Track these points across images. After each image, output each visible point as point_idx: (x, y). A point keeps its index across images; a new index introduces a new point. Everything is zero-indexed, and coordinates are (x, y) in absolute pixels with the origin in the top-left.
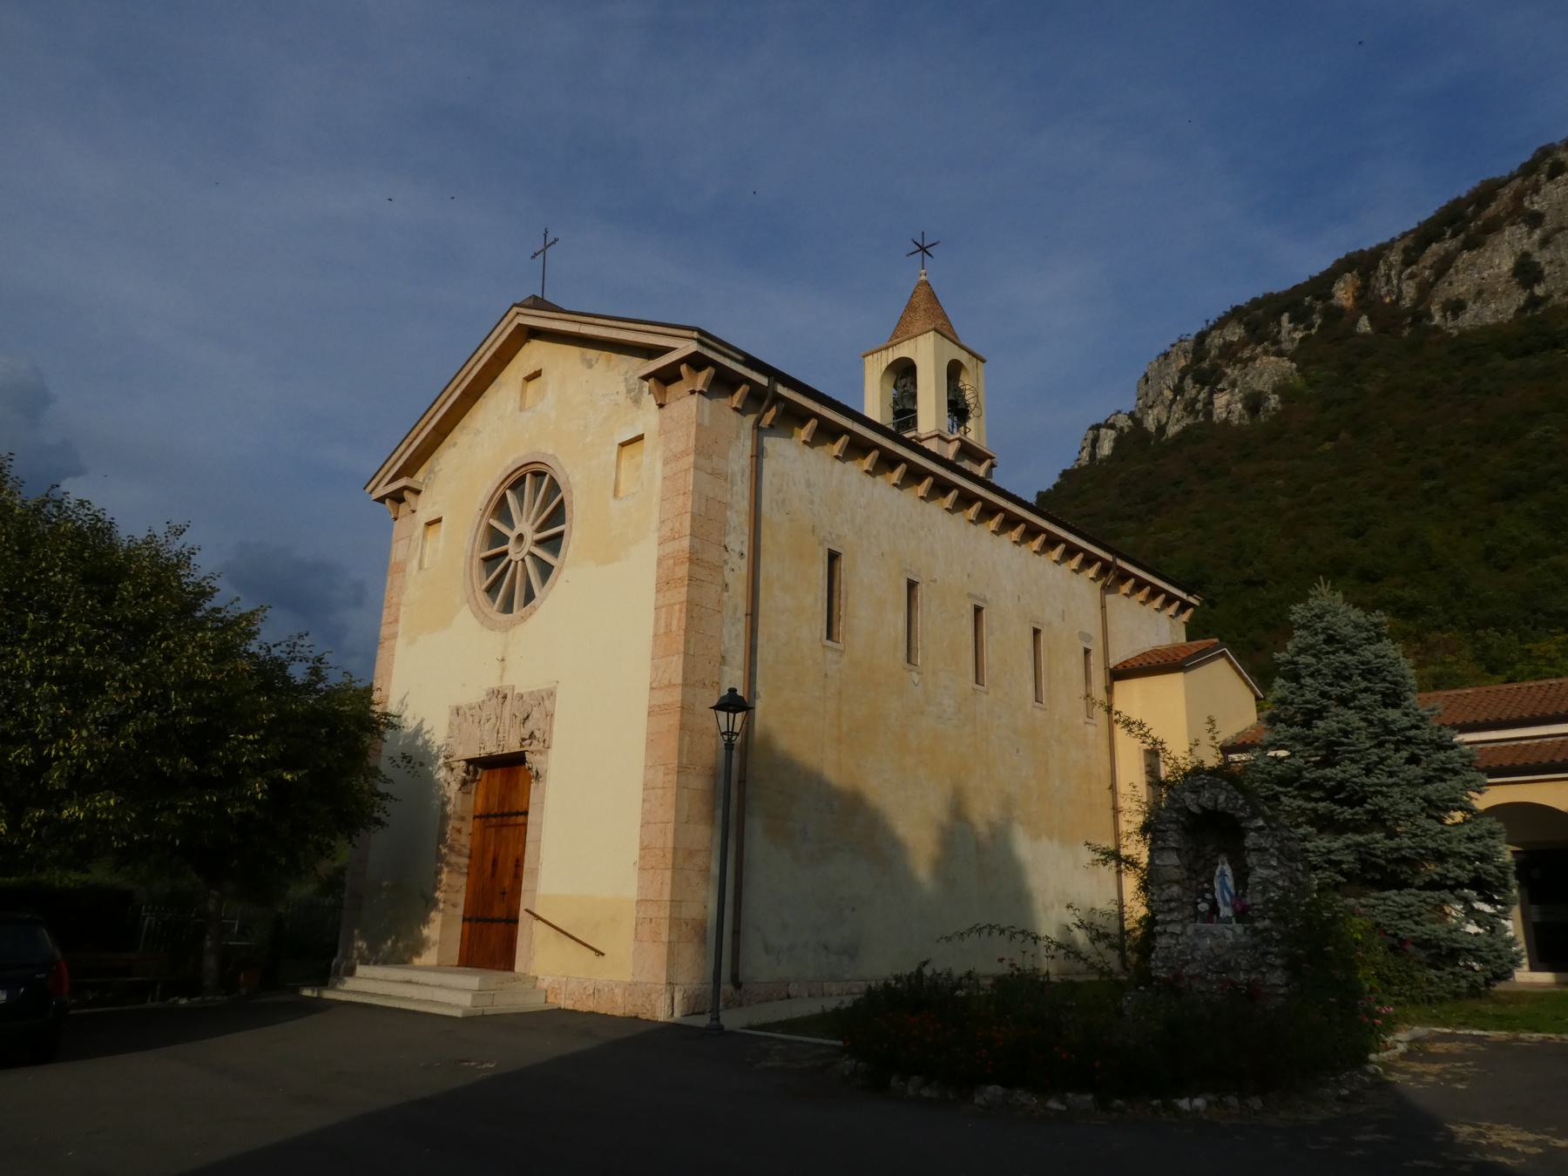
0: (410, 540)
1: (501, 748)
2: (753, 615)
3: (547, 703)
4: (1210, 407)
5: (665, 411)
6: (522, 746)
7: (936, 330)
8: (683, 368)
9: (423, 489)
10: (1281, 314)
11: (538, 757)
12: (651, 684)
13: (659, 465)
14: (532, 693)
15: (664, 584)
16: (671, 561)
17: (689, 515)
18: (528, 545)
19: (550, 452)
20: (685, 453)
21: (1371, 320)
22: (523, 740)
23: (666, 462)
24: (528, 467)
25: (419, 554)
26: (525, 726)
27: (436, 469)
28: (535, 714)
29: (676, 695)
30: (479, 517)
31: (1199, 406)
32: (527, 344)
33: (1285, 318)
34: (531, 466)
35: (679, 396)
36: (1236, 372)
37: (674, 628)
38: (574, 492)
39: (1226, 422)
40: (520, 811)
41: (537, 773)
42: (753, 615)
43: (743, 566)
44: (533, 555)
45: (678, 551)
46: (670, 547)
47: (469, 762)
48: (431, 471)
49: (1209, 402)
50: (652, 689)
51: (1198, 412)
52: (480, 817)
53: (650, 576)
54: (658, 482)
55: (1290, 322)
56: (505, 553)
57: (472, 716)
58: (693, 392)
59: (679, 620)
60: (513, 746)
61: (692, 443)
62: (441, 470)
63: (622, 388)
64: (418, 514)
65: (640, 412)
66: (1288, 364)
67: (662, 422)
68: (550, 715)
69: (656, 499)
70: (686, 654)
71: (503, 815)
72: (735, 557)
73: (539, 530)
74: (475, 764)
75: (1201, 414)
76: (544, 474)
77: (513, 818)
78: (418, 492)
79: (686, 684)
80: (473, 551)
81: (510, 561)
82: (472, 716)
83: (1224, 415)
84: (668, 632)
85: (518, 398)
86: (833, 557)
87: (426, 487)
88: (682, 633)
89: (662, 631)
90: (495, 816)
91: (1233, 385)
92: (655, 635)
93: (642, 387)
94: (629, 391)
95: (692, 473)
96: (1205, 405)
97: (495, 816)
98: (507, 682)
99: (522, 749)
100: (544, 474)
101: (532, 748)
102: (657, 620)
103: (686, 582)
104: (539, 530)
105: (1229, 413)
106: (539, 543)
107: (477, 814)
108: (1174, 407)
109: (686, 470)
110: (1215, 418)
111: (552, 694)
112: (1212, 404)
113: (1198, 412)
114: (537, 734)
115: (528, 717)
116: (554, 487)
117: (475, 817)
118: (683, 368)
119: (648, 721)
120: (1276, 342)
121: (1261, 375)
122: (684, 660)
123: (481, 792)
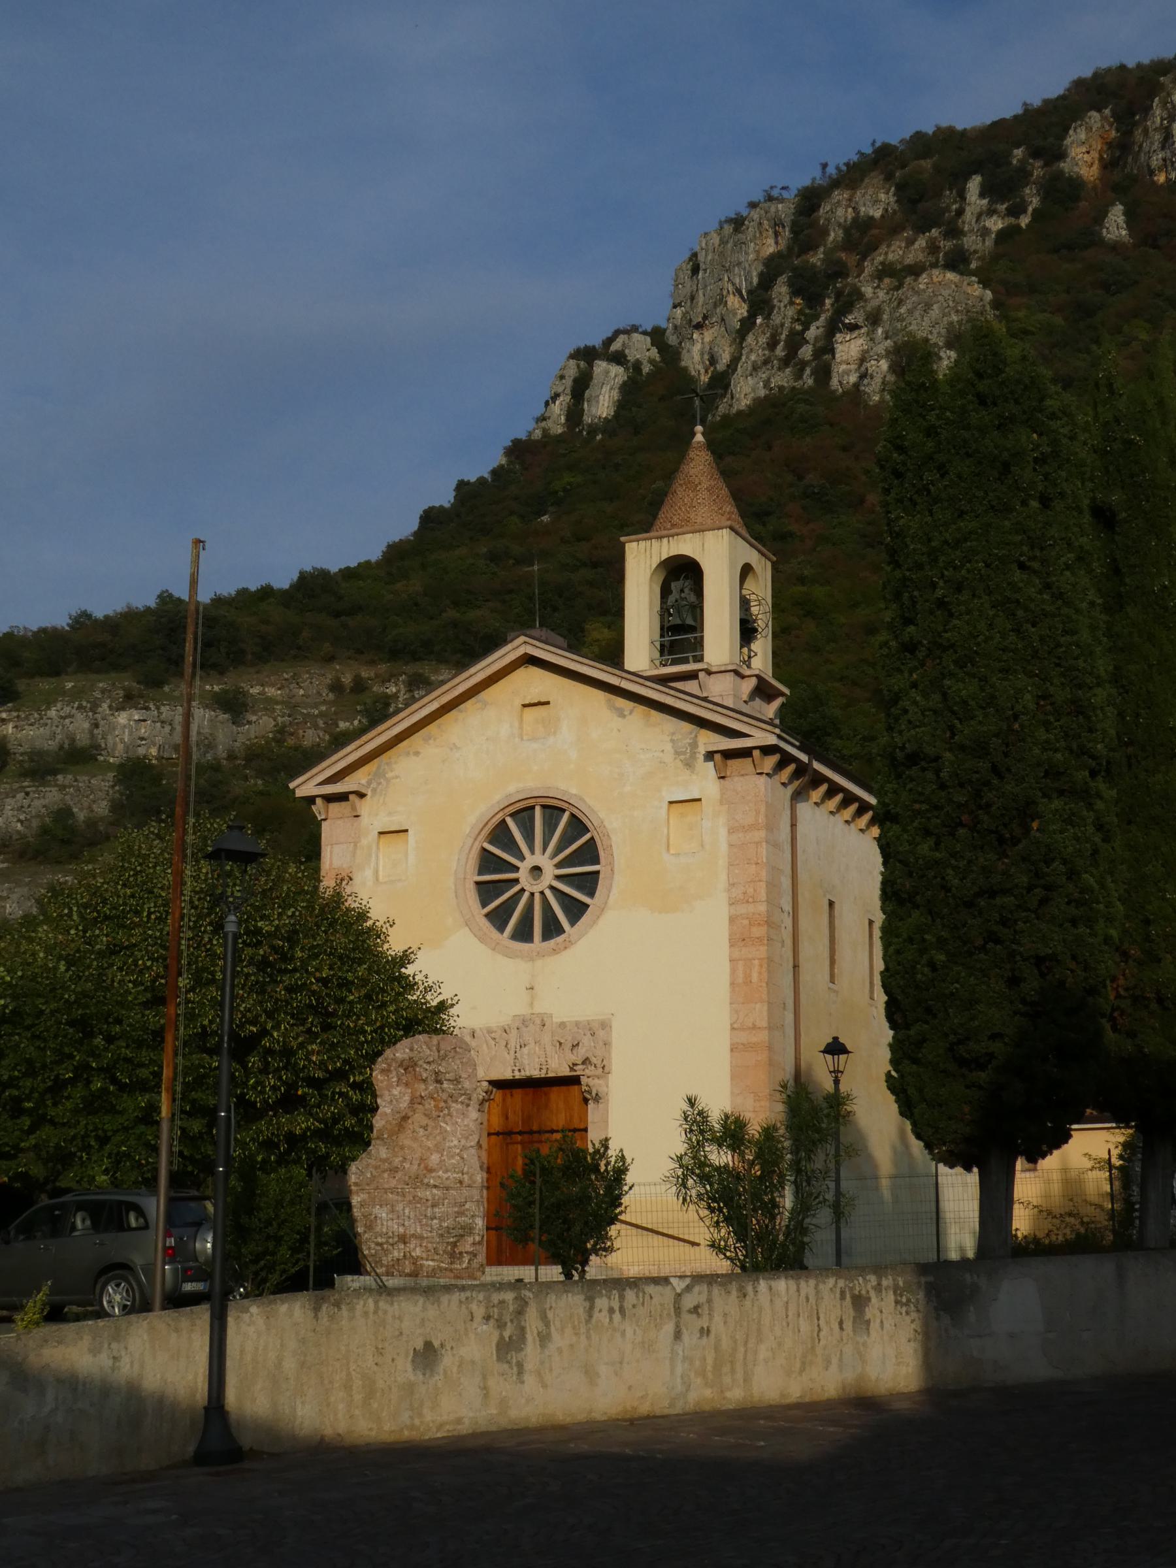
0: (356, 845)
1: (544, 1071)
2: (796, 967)
3: (601, 1034)
4: (827, 357)
5: (726, 782)
6: (572, 1069)
7: (732, 528)
8: (756, 753)
9: (369, 793)
10: (967, 177)
11: (596, 1081)
12: (731, 1025)
13: (723, 832)
14: (577, 1024)
15: (738, 940)
16: (746, 922)
17: (763, 885)
18: (548, 878)
19: (574, 791)
20: (752, 827)
21: (1130, 215)
22: (577, 1065)
23: (732, 831)
24: (539, 800)
25: (373, 864)
26: (574, 1052)
27: (390, 775)
28: (586, 1041)
29: (763, 1037)
30: (472, 840)
31: (806, 352)
32: (522, 669)
33: (974, 185)
34: (575, 810)
35: (742, 772)
36: (881, 294)
37: (755, 977)
38: (614, 838)
39: (855, 393)
40: (555, 1128)
41: (597, 1094)
42: (796, 967)
43: (788, 922)
44: (552, 888)
45: (754, 914)
46: (742, 909)
47: (491, 1082)
48: (379, 775)
49: (826, 349)
50: (733, 1029)
51: (803, 365)
52: (497, 1134)
53: (721, 932)
54: (723, 847)
55: (982, 195)
56: (516, 881)
57: (494, 1039)
58: (761, 774)
59: (760, 973)
60: (559, 1067)
61: (761, 819)
62: (397, 777)
63: (669, 747)
64: (365, 820)
65: (694, 777)
66: (976, 290)
67: (723, 792)
68: (607, 1044)
69: (722, 862)
70: (769, 1003)
71: (531, 1132)
72: (786, 914)
73: (559, 865)
74: (499, 1084)
75: (808, 371)
76: (563, 811)
77: (547, 1135)
78: (362, 795)
79: (770, 1028)
80: (465, 872)
81: (523, 890)
82: (494, 1039)
83: (853, 379)
84: (748, 981)
85: (516, 724)
86: (831, 904)
87: (374, 790)
88: (764, 985)
89: (740, 980)
90: (520, 1133)
91: (874, 319)
92: (732, 984)
93: (695, 753)
94: (677, 753)
95: (764, 846)
96: (818, 353)
97: (520, 1133)
98: (538, 1009)
99: (575, 1074)
100: (563, 811)
101: (587, 1072)
102: (733, 971)
103: (766, 942)
104: (559, 865)
105: (863, 376)
106: (558, 877)
107: (493, 1131)
108: (750, 339)
109: (757, 843)
110: (834, 382)
111: (605, 1025)
112: (832, 351)
113: (803, 365)
114: (594, 1060)
115: (578, 1044)
116: (578, 826)
117: (489, 1134)
118: (756, 753)
119: (731, 1057)
120: (954, 232)
121: (928, 306)
122: (769, 1010)
123: (496, 1110)
